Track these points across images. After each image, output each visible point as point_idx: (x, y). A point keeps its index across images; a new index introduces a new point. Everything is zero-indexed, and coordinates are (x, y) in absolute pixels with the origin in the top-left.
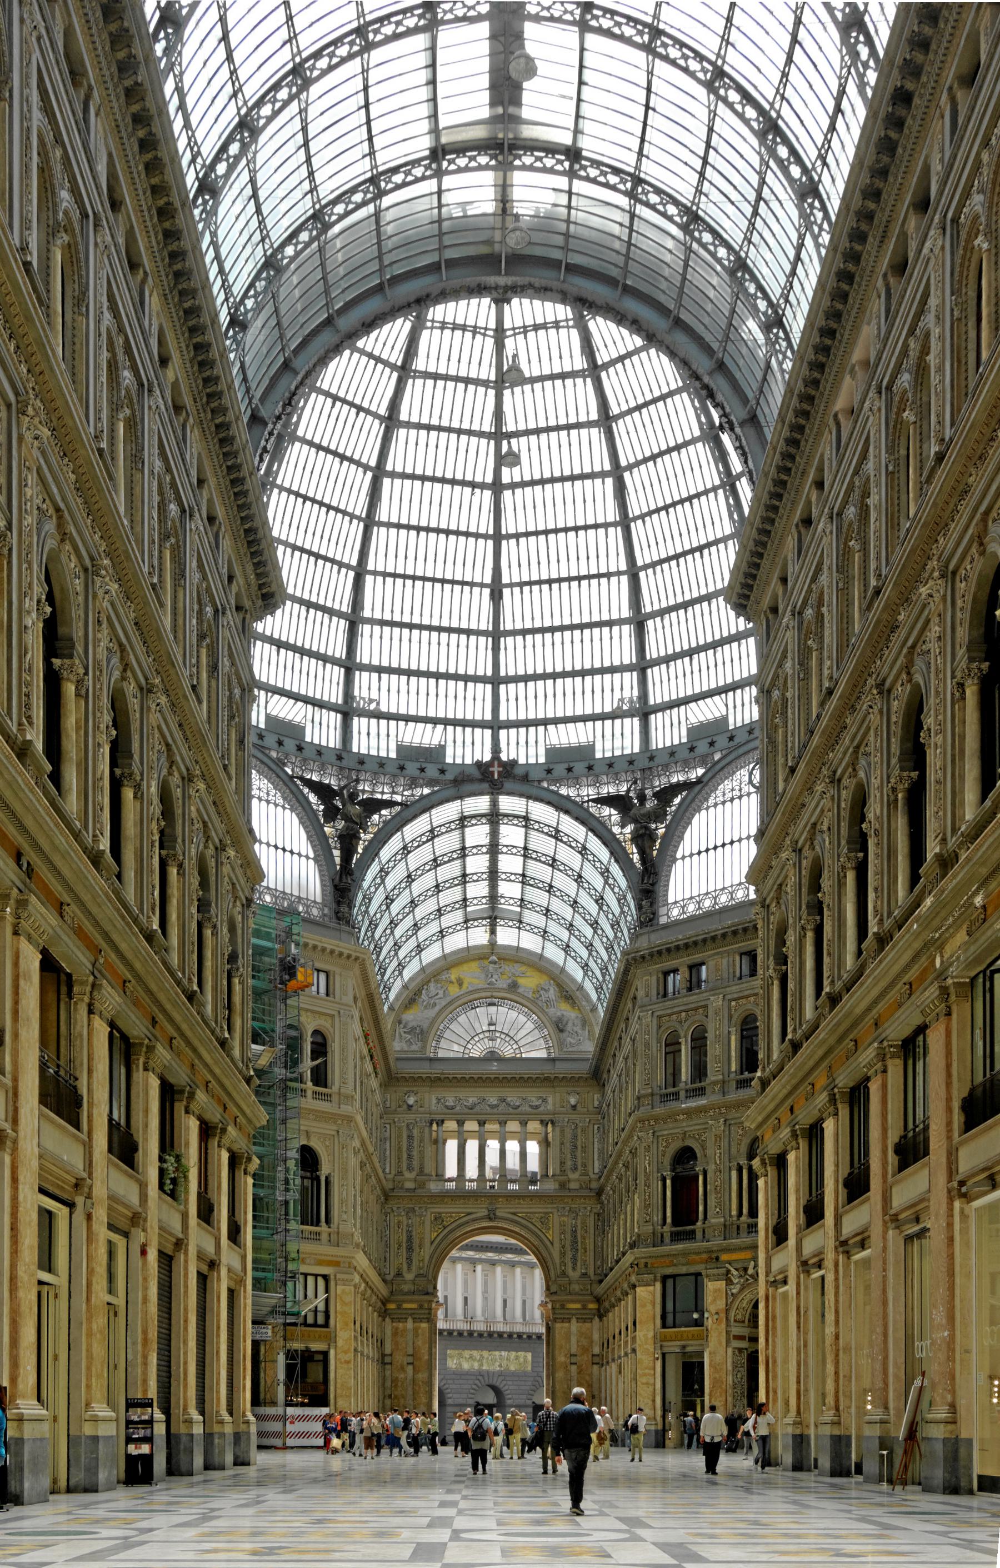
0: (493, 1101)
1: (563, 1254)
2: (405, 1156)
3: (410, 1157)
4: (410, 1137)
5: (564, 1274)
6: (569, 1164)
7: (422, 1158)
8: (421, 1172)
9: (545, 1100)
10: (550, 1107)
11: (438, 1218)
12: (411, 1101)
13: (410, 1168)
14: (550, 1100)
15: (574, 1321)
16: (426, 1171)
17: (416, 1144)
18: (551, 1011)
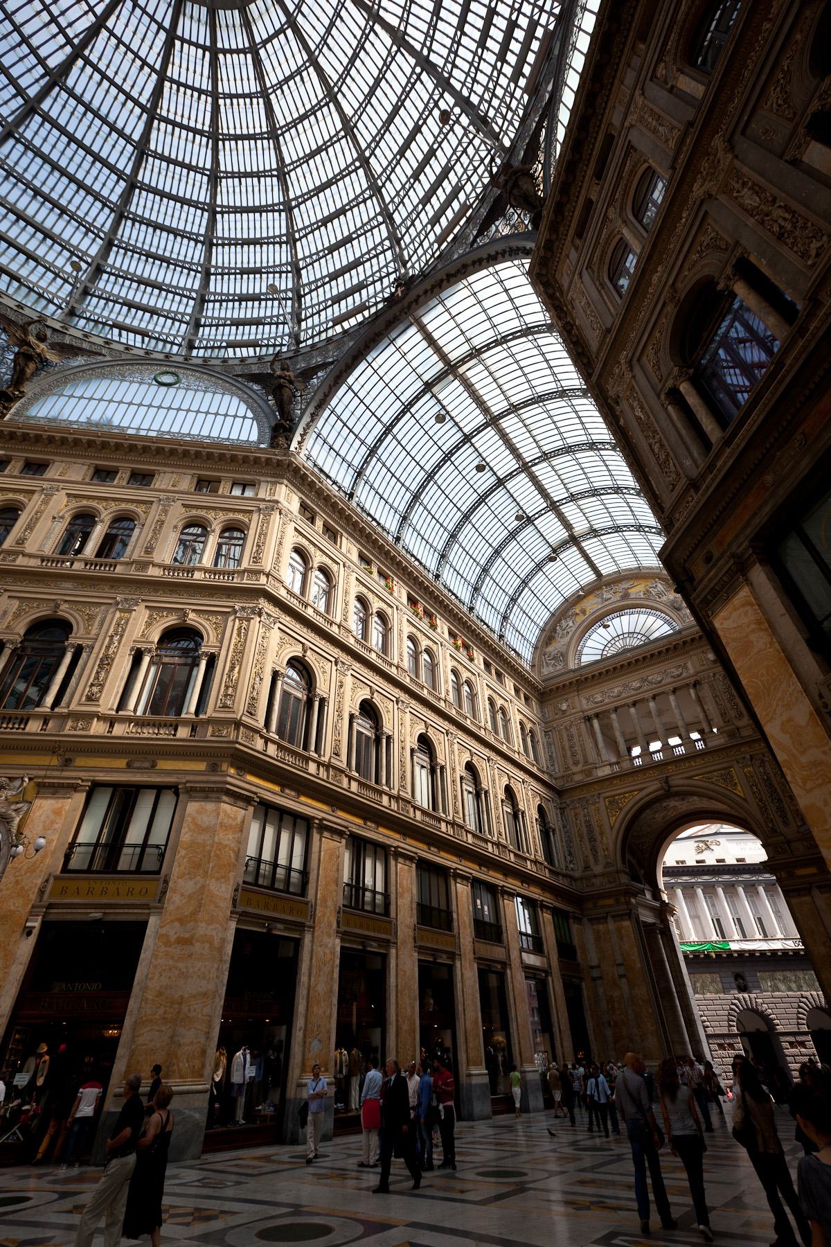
0: (636, 684)
1: (763, 809)
2: (569, 754)
3: (573, 755)
4: (571, 737)
5: (774, 830)
6: (732, 713)
7: (584, 750)
8: (586, 762)
9: (685, 667)
10: (692, 671)
11: (613, 802)
12: (564, 707)
13: (576, 763)
14: (689, 665)
15: (816, 892)
16: (591, 761)
17: (576, 739)
18: (664, 598)
